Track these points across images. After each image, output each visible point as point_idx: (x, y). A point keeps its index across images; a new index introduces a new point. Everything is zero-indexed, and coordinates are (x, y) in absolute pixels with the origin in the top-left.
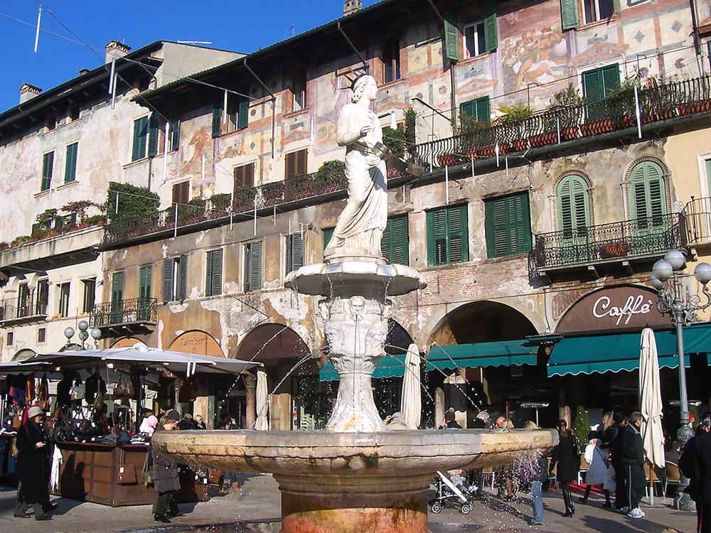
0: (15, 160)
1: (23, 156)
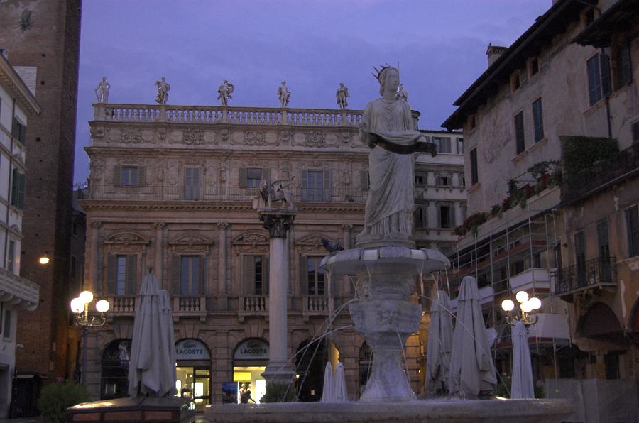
0: (492, 128)
1: (498, 121)
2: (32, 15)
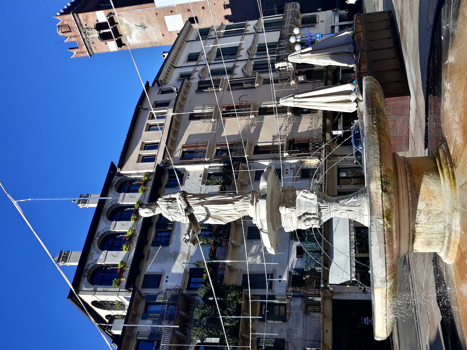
2: (137, 25)
